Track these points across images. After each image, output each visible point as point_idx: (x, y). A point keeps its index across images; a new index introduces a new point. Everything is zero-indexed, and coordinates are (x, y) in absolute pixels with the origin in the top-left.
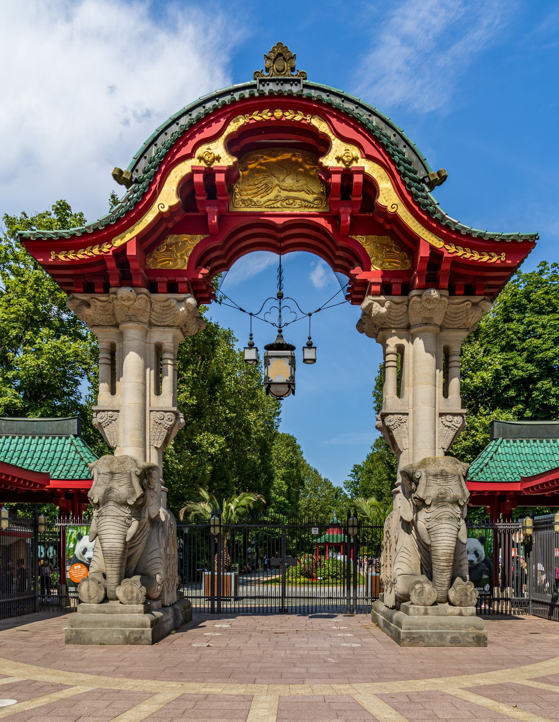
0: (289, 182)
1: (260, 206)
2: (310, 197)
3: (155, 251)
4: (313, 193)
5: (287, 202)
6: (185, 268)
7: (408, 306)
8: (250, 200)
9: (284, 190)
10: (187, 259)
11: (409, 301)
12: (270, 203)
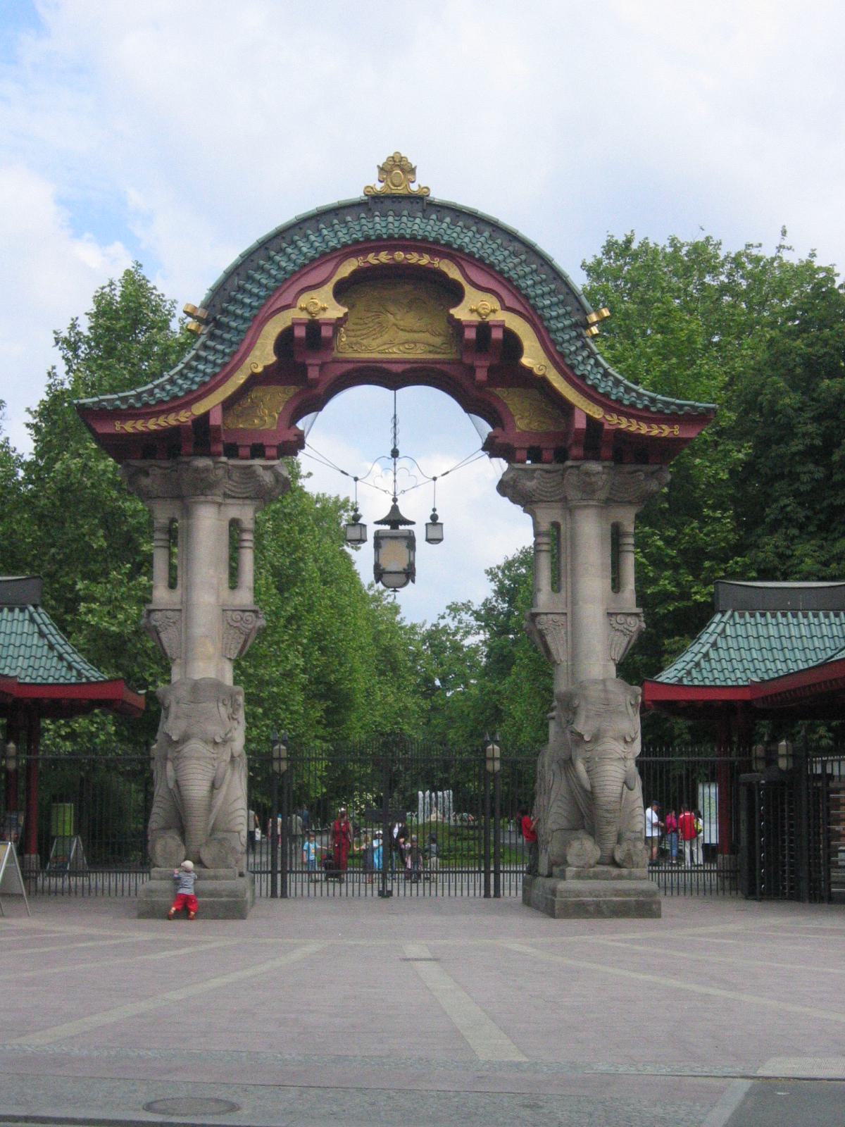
0: (410, 320)
2: (438, 341)
3: (235, 407)
4: (440, 335)
5: (407, 346)
6: (274, 428)
7: (562, 475)
8: (360, 344)
9: (402, 330)
10: (277, 416)
11: (565, 470)
12: (385, 347)
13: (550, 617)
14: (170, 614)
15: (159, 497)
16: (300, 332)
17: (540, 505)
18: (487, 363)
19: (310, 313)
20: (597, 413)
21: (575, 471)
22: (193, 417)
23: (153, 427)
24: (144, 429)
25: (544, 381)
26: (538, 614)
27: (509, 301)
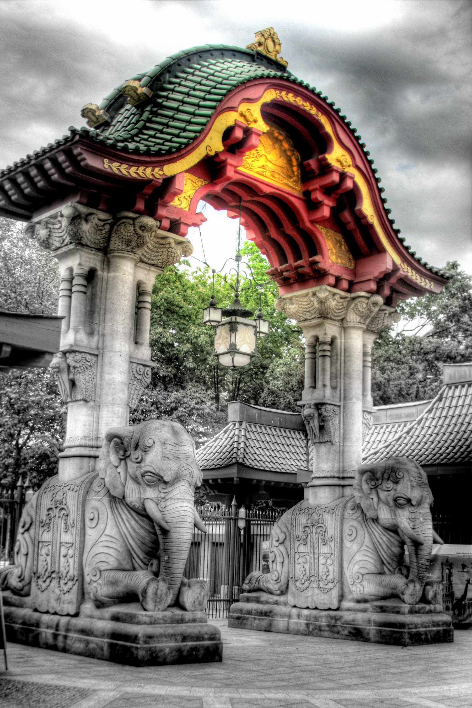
1: (251, 169)
13: (332, 407)
14: (88, 357)
15: (87, 246)
16: (239, 134)
17: (329, 321)
18: (331, 204)
19: (247, 121)
20: (398, 260)
21: (366, 301)
22: (164, 177)
23: (134, 175)
24: (127, 174)
25: (371, 226)
26: (323, 404)
27: (359, 162)
